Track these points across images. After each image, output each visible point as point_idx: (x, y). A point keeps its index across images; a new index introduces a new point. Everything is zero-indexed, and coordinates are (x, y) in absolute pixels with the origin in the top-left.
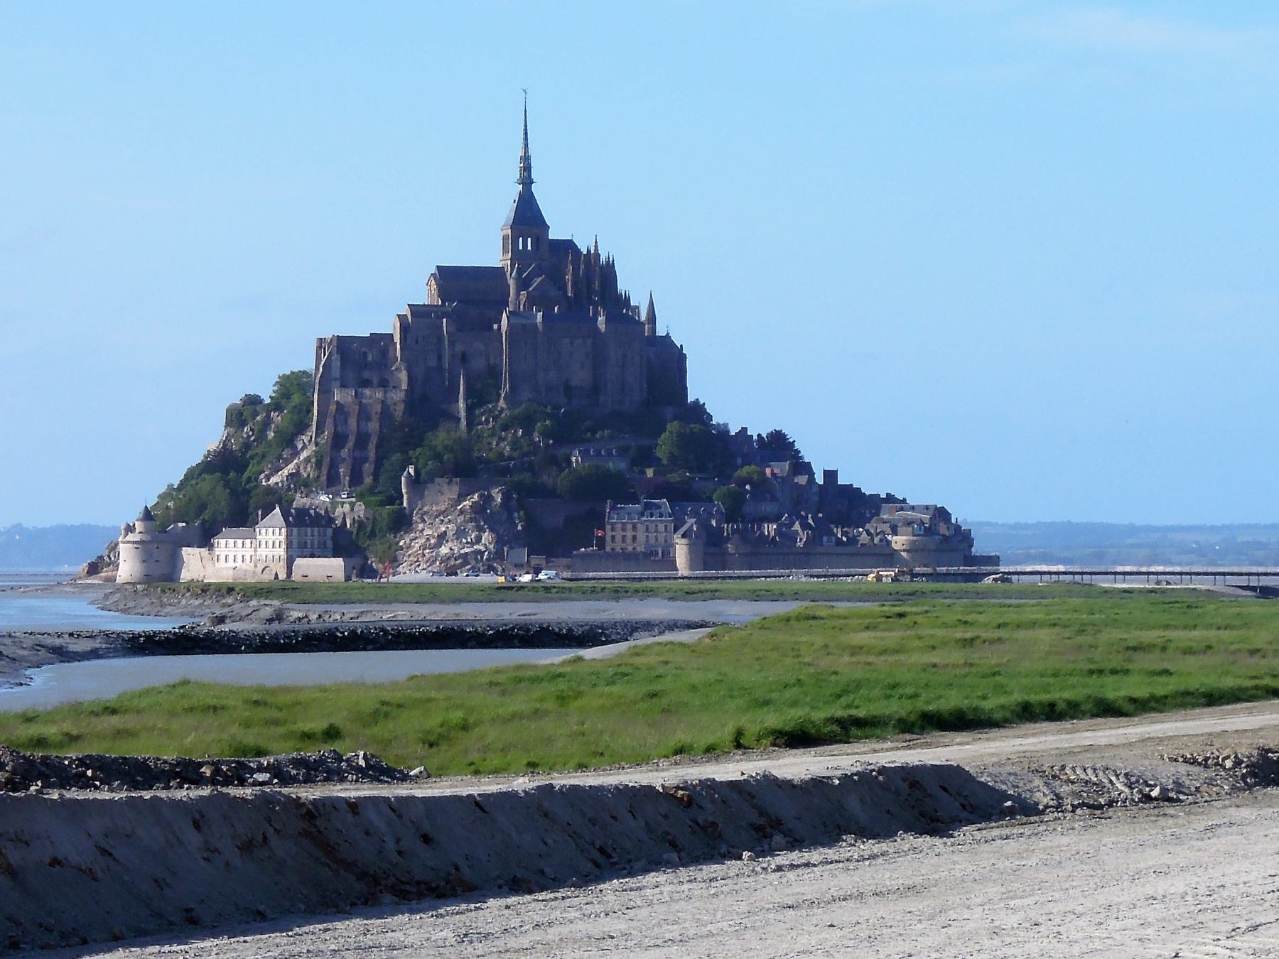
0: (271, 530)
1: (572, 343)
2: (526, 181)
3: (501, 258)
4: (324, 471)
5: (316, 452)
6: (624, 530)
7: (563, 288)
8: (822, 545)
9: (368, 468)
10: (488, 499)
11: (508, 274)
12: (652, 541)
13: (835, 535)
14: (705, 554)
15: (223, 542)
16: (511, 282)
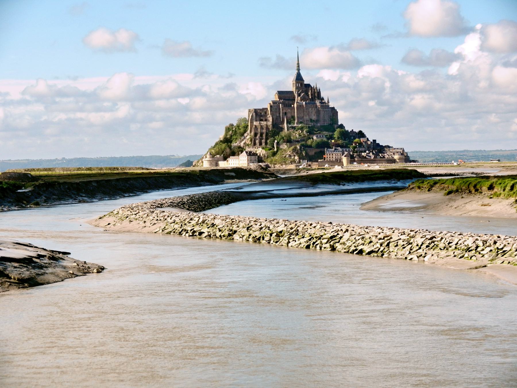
0: (243, 157)
1: (312, 109)
2: (299, 70)
3: (292, 88)
4: (253, 142)
5: (250, 138)
6: (330, 155)
7: (308, 96)
8: (377, 158)
9: (263, 141)
10: (296, 148)
11: (295, 93)
12: (337, 158)
13: (380, 155)
14: (350, 161)
15: (230, 160)
16: (296, 95)
